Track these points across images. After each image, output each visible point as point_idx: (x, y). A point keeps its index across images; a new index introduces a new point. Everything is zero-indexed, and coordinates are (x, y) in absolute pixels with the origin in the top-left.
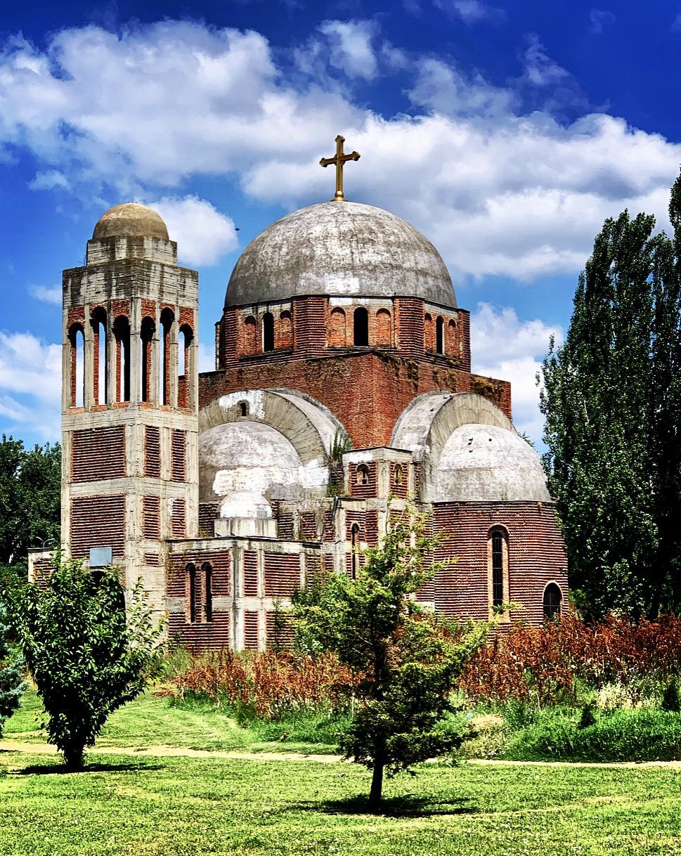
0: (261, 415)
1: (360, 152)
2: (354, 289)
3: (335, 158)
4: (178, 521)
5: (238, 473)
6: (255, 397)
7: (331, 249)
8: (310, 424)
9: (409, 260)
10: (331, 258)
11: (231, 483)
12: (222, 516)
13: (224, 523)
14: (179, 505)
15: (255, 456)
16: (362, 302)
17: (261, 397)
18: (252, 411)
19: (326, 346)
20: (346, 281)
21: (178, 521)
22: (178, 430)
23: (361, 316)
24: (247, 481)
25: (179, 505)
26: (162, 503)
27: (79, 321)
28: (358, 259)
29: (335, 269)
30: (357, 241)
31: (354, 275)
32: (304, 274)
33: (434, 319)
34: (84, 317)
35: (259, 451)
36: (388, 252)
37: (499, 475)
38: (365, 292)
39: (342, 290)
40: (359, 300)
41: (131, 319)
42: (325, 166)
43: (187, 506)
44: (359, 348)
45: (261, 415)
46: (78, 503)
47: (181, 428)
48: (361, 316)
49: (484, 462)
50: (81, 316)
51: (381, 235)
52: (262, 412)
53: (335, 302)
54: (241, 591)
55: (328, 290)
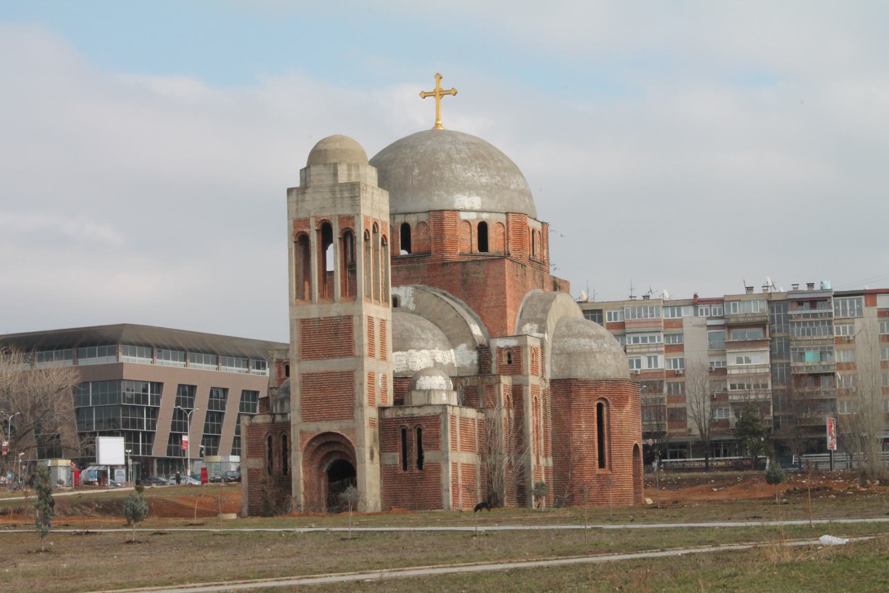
0: (412, 307)
1: (457, 89)
2: (477, 206)
3: (435, 91)
4: (384, 391)
5: (410, 354)
6: (406, 292)
7: (457, 171)
8: (458, 315)
9: (513, 183)
10: (458, 180)
11: (404, 362)
12: (418, 388)
13: (421, 394)
14: (384, 377)
15: (421, 340)
16: (485, 217)
17: (411, 292)
18: (403, 303)
19: (459, 251)
20: (470, 199)
21: (384, 391)
22: (383, 320)
23: (483, 228)
24: (418, 361)
25: (384, 377)
26: (376, 376)
27: (305, 230)
28: (478, 181)
29: (462, 188)
30: (475, 165)
31: (478, 195)
32: (436, 192)
33: (531, 230)
34: (309, 227)
35: (423, 336)
36: (499, 175)
37: (600, 357)
38: (486, 207)
39: (468, 207)
40: (481, 214)
41: (357, 230)
42: (424, 98)
43: (388, 380)
44: (482, 253)
45: (412, 307)
46: (307, 378)
47: (384, 318)
48: (483, 228)
49: (588, 348)
50: (306, 226)
51: (492, 162)
52: (412, 304)
53: (464, 216)
54: (681, 430)
55: (457, 205)
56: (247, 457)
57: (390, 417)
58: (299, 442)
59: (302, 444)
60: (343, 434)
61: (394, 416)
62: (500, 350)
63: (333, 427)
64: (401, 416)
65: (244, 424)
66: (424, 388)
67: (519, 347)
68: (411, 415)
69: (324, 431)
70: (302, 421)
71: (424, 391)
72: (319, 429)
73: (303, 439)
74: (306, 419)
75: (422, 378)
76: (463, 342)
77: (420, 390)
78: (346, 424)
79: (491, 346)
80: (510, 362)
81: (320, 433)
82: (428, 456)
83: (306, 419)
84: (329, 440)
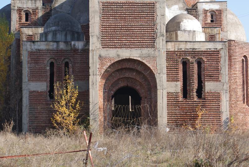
56: (29, 80)
57: (173, 50)
58: (98, 66)
59: (100, 69)
60: (144, 61)
61: (176, 50)
62: (206, 11)
63: (134, 54)
64: (183, 49)
65: (27, 50)
66: (188, 29)
67: (221, 10)
68: (193, 49)
69: (124, 58)
70: (101, 47)
71: (189, 31)
72: (118, 55)
73: (102, 64)
74: (105, 46)
75: (185, 21)
76: (175, 4)
77: (185, 31)
78: (145, 51)
79: (198, 8)
80: (212, 21)
81: (120, 59)
82: (209, 86)
83: (105, 46)
84: (124, 67)
